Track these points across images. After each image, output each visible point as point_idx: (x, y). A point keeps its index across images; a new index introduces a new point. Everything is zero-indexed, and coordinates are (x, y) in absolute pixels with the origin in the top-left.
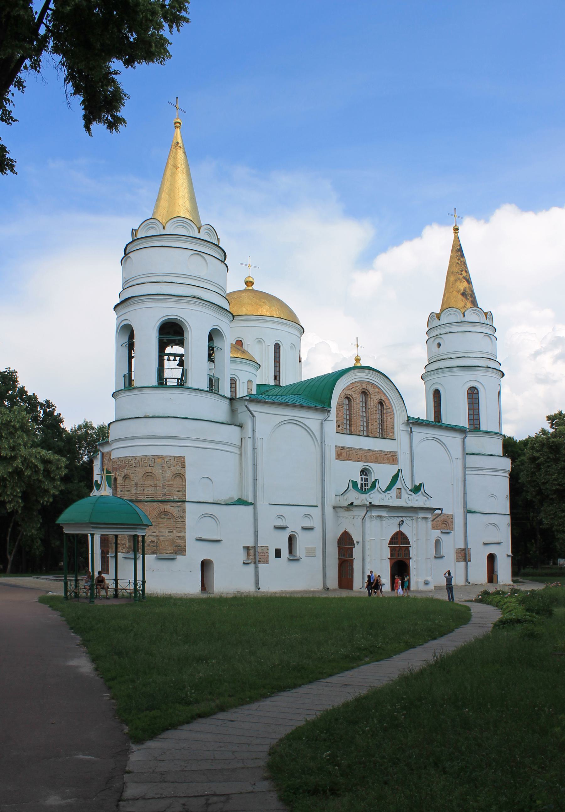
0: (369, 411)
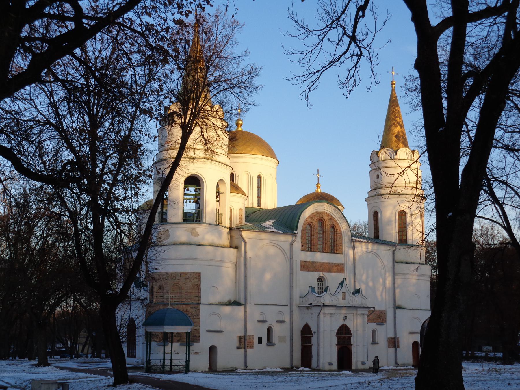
0: (324, 234)
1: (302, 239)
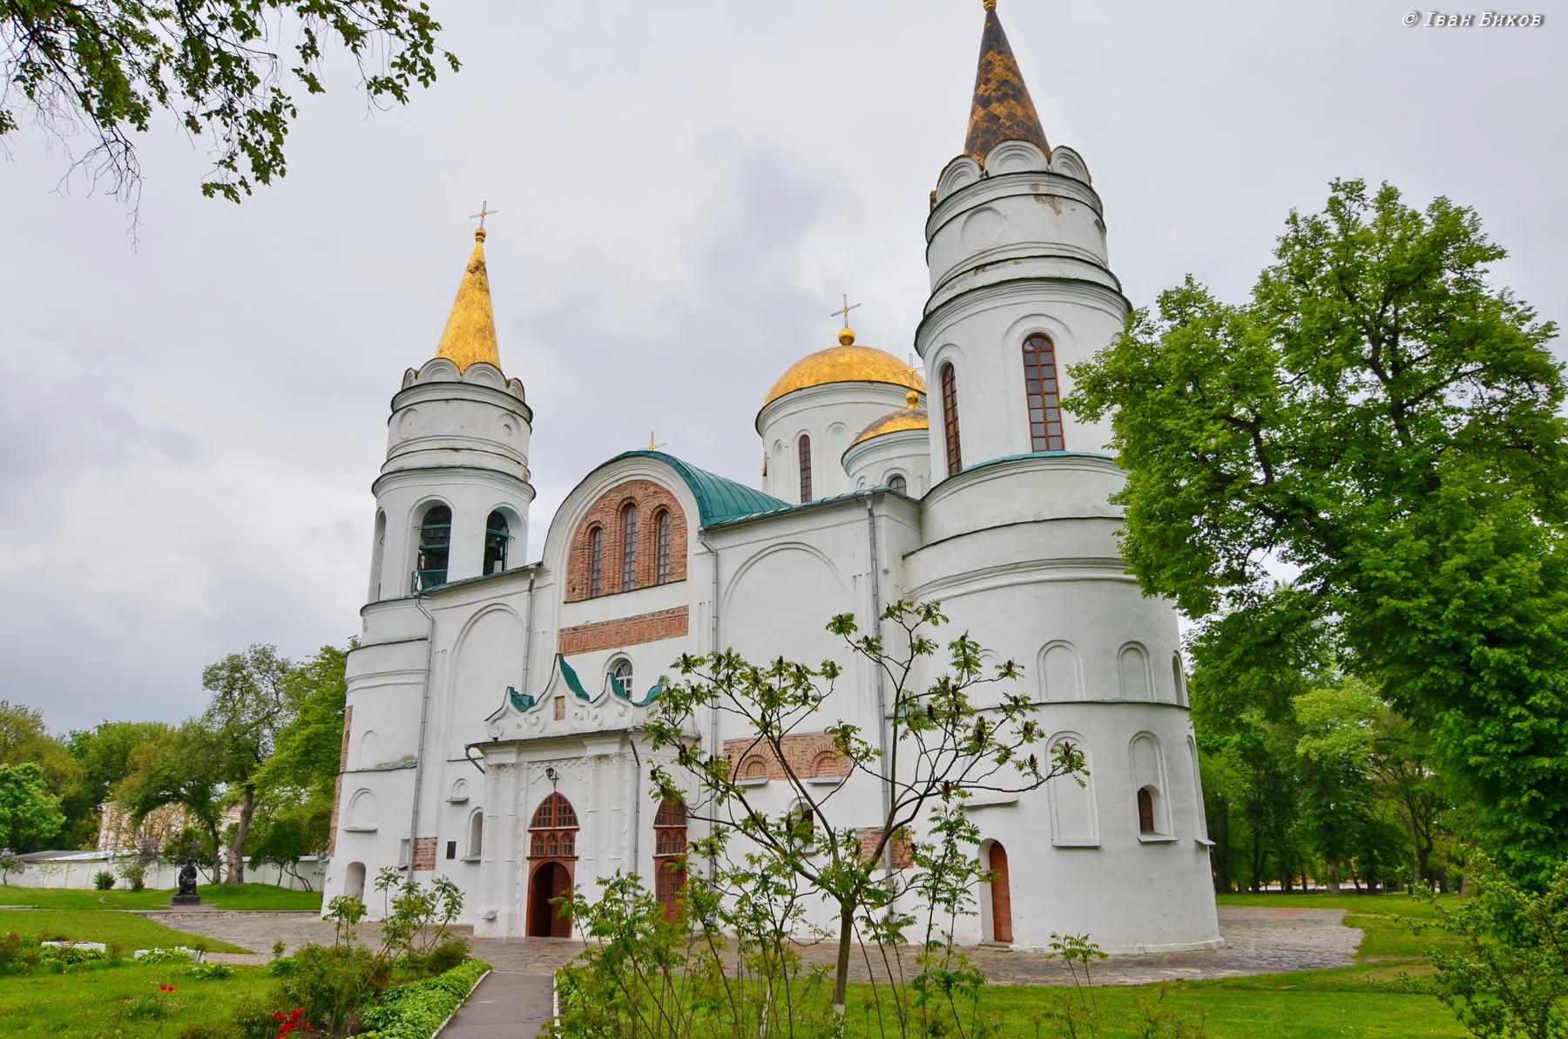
1: (570, 572)
